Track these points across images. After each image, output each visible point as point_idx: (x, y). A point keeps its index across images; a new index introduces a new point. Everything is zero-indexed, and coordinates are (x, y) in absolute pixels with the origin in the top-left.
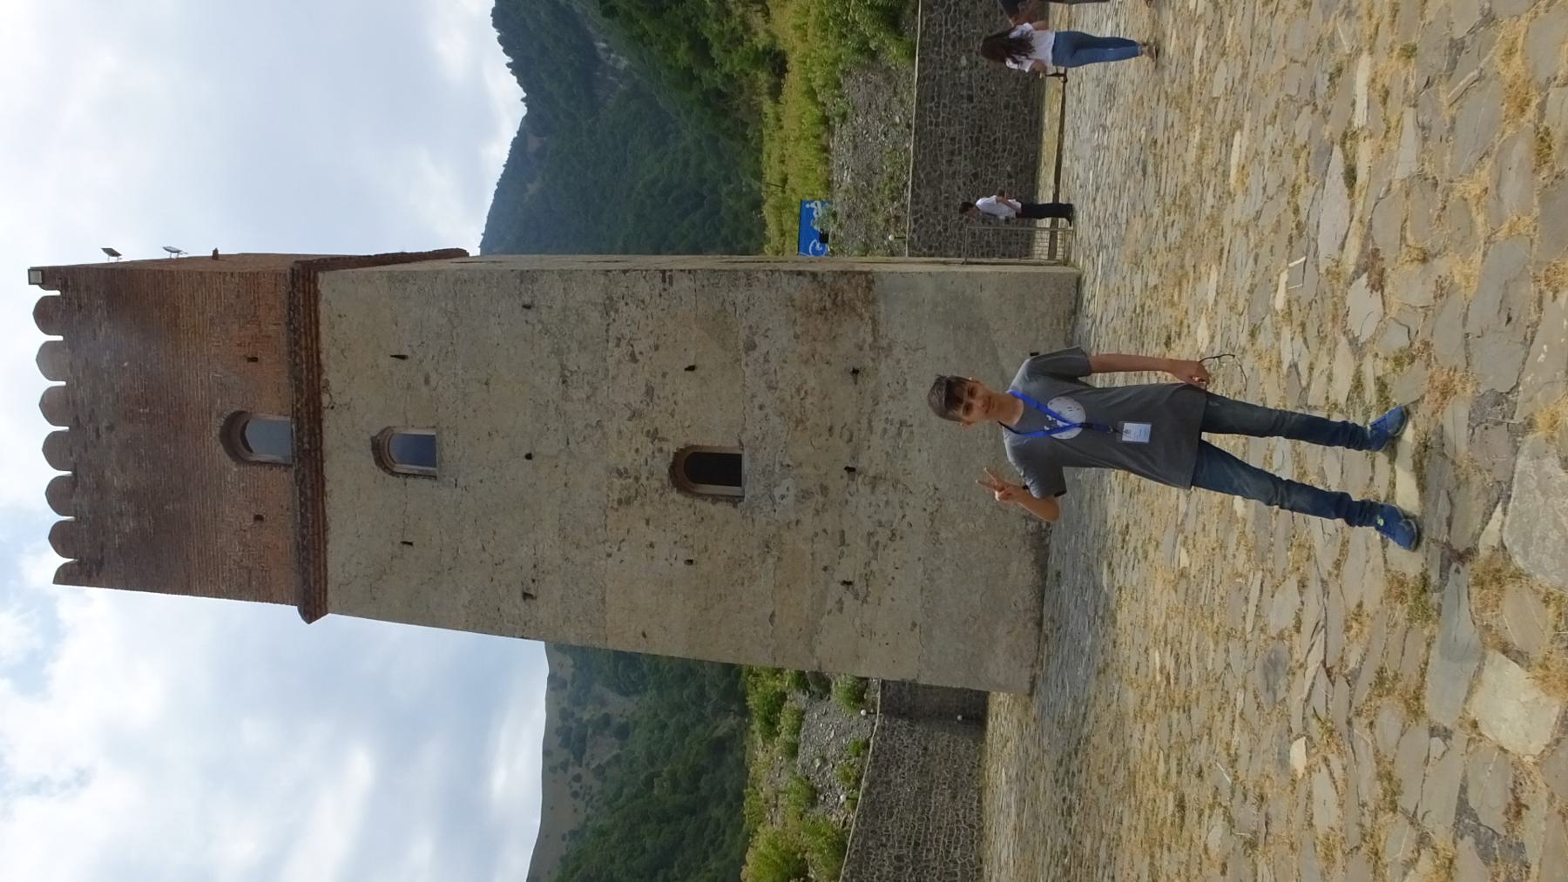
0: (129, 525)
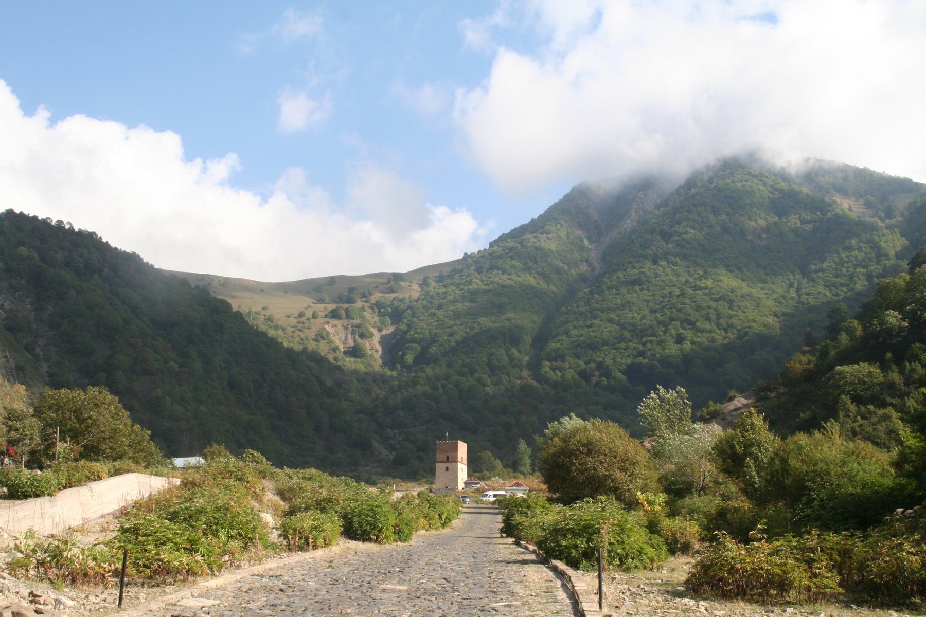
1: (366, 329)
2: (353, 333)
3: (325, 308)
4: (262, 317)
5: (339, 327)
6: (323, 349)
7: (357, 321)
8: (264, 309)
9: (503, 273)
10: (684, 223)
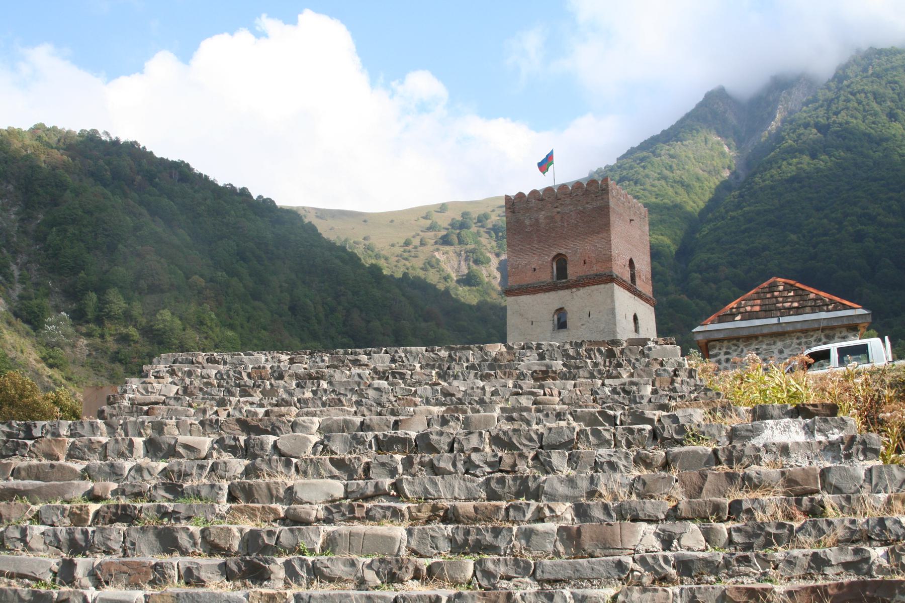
0: (527, 222)
1: (482, 254)
2: (467, 259)
3: (436, 236)
4: (362, 247)
5: (451, 254)
6: (432, 277)
7: (470, 247)
8: (365, 239)
9: (636, 183)
10: (843, 113)
